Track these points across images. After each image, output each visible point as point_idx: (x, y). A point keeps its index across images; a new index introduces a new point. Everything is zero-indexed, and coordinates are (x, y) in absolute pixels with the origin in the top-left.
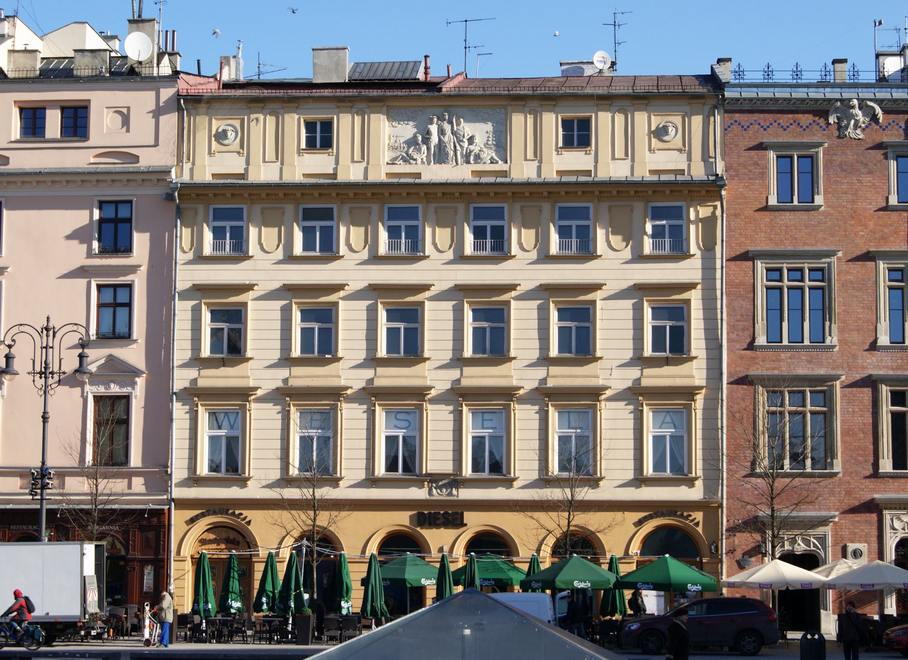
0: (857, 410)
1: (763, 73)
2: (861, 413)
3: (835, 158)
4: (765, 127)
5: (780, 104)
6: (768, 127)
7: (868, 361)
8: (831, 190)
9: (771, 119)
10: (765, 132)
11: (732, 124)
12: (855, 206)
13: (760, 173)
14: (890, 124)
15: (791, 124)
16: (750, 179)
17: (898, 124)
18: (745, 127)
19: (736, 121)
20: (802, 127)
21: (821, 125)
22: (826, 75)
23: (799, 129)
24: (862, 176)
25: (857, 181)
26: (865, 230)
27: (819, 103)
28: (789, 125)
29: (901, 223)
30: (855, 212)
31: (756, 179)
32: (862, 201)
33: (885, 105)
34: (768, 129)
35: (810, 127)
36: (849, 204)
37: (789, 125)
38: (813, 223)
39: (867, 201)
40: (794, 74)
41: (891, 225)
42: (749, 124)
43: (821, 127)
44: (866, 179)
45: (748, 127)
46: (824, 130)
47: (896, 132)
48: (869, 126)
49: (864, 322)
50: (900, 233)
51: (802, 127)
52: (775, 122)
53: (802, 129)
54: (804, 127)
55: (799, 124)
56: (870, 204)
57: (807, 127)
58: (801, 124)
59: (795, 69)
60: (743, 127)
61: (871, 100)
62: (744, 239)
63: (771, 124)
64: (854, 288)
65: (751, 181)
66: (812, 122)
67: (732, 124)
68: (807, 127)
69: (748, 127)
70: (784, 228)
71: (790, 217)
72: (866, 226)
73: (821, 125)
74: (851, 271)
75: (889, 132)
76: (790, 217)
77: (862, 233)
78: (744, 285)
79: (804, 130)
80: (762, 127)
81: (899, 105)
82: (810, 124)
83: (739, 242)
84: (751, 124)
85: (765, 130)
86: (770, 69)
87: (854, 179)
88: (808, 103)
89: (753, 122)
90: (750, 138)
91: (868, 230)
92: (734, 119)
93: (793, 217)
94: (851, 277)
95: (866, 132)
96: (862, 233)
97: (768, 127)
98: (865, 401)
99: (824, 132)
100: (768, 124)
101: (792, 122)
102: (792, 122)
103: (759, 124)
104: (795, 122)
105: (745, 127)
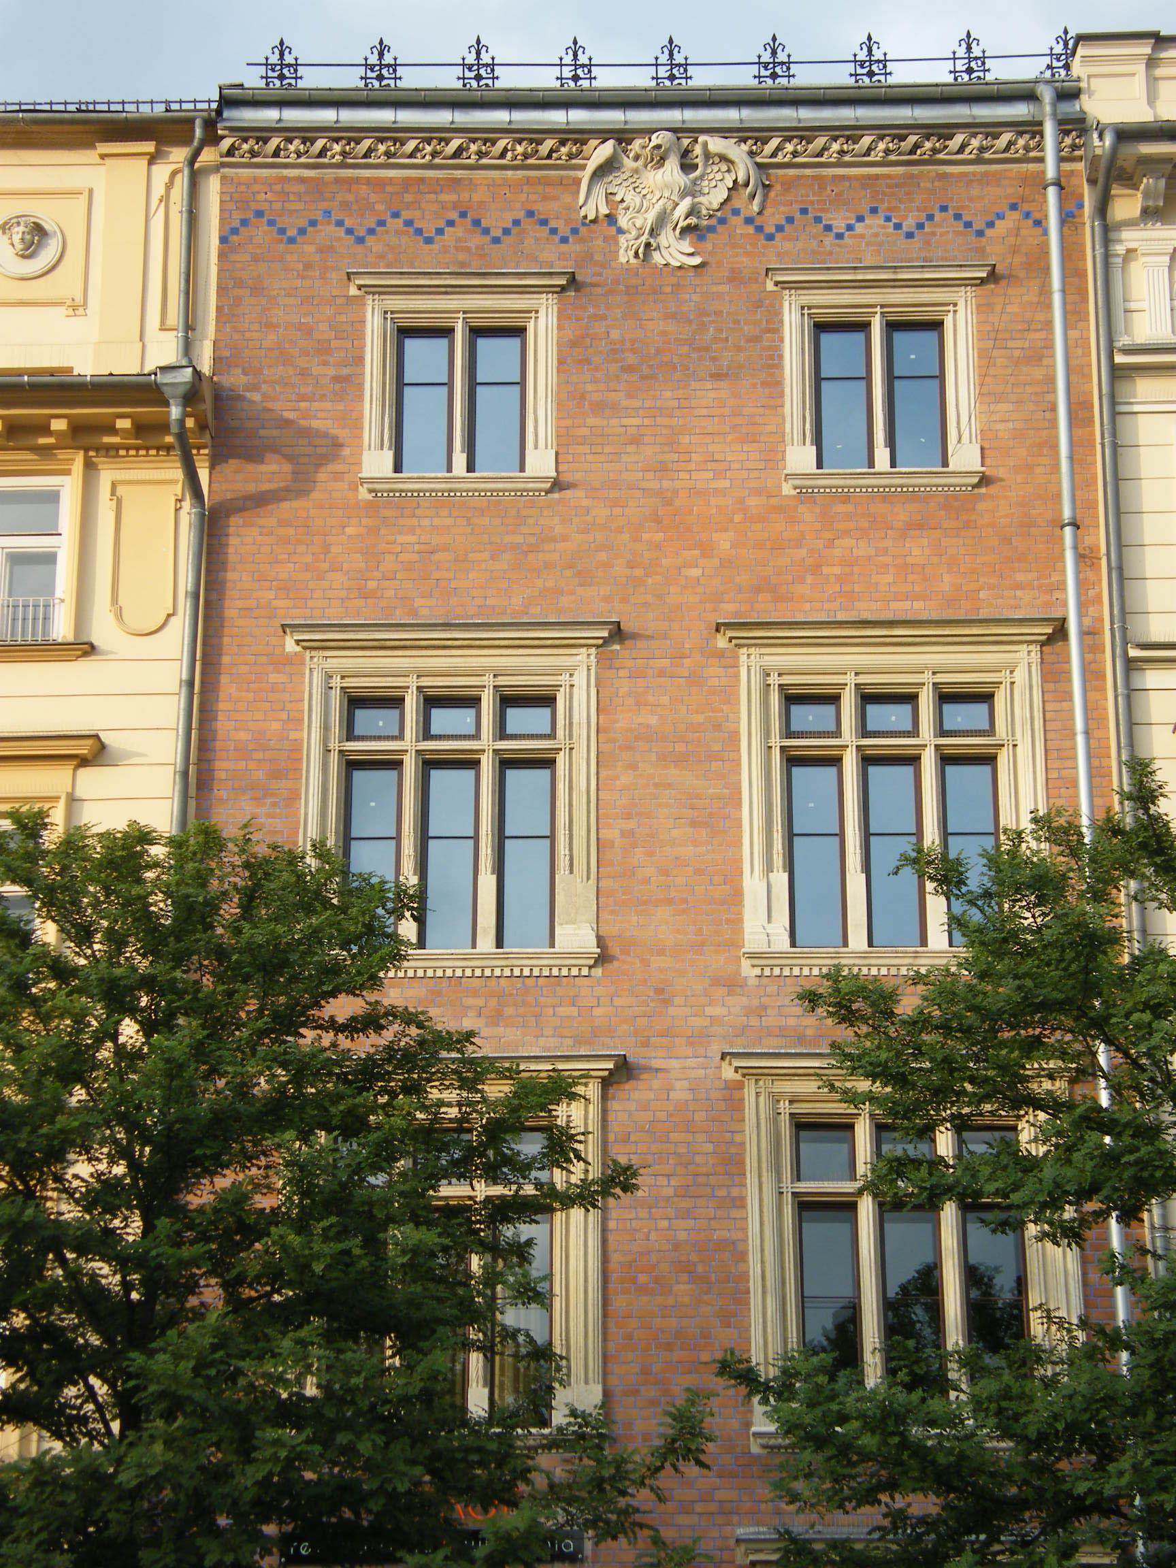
0: (669, 1192)
1: (361, 71)
2: (686, 1204)
3: (600, 328)
4: (361, 232)
5: (411, 156)
6: (371, 231)
7: (709, 1011)
8: (586, 431)
9: (380, 207)
10: (359, 249)
11: (244, 222)
12: (666, 484)
13: (336, 379)
14: (790, 220)
15: (451, 223)
16: (303, 398)
17: (818, 220)
18: (289, 233)
19: (259, 214)
20: (486, 231)
21: (553, 224)
22: (576, 78)
23: (476, 240)
24: (693, 385)
25: (675, 404)
26: (701, 562)
27: (545, 148)
28: (441, 224)
29: (828, 535)
30: (668, 503)
31: (323, 398)
32: (692, 466)
33: (774, 155)
34: (370, 241)
35: (515, 230)
36: (650, 475)
37: (441, 224)
38: (520, 539)
39: (710, 466)
40: (468, 74)
41: (799, 544)
42: (303, 222)
43: (554, 231)
44: (708, 395)
45: (302, 231)
46: (564, 240)
47: (814, 244)
48: (720, 228)
49: (698, 872)
50: (825, 570)
51: (486, 231)
52: (396, 215)
53: (487, 239)
54: (497, 233)
55: (477, 223)
56: (718, 475)
57: (506, 231)
58: (484, 224)
59: (471, 59)
60: (282, 231)
61: (723, 132)
62: (271, 594)
63: (382, 223)
64: (663, 758)
65: (303, 405)
66: (520, 215)
67: (244, 222)
68: (506, 231)
69: (302, 231)
70: (416, 557)
71: (436, 522)
72: (706, 549)
73: (553, 224)
74: (651, 699)
75: (788, 245)
76: (436, 522)
77: (695, 572)
78: (265, 749)
79: (496, 240)
80: (350, 231)
81: (820, 155)
82: (517, 222)
83: (252, 603)
84: (313, 223)
85: (360, 240)
86: (388, 59)
87: (668, 394)
88: (505, 150)
89: (319, 216)
90: (308, 266)
91: (716, 562)
92: (253, 206)
93: (449, 521)
94: (653, 720)
95: (708, 246)
96: (695, 572)
97: (371, 231)
98: (698, 1159)
99: (564, 247)
100: (371, 222)
101: (454, 215)
102: (454, 215)
103: (340, 223)
104: (463, 215)
105: (292, 232)
